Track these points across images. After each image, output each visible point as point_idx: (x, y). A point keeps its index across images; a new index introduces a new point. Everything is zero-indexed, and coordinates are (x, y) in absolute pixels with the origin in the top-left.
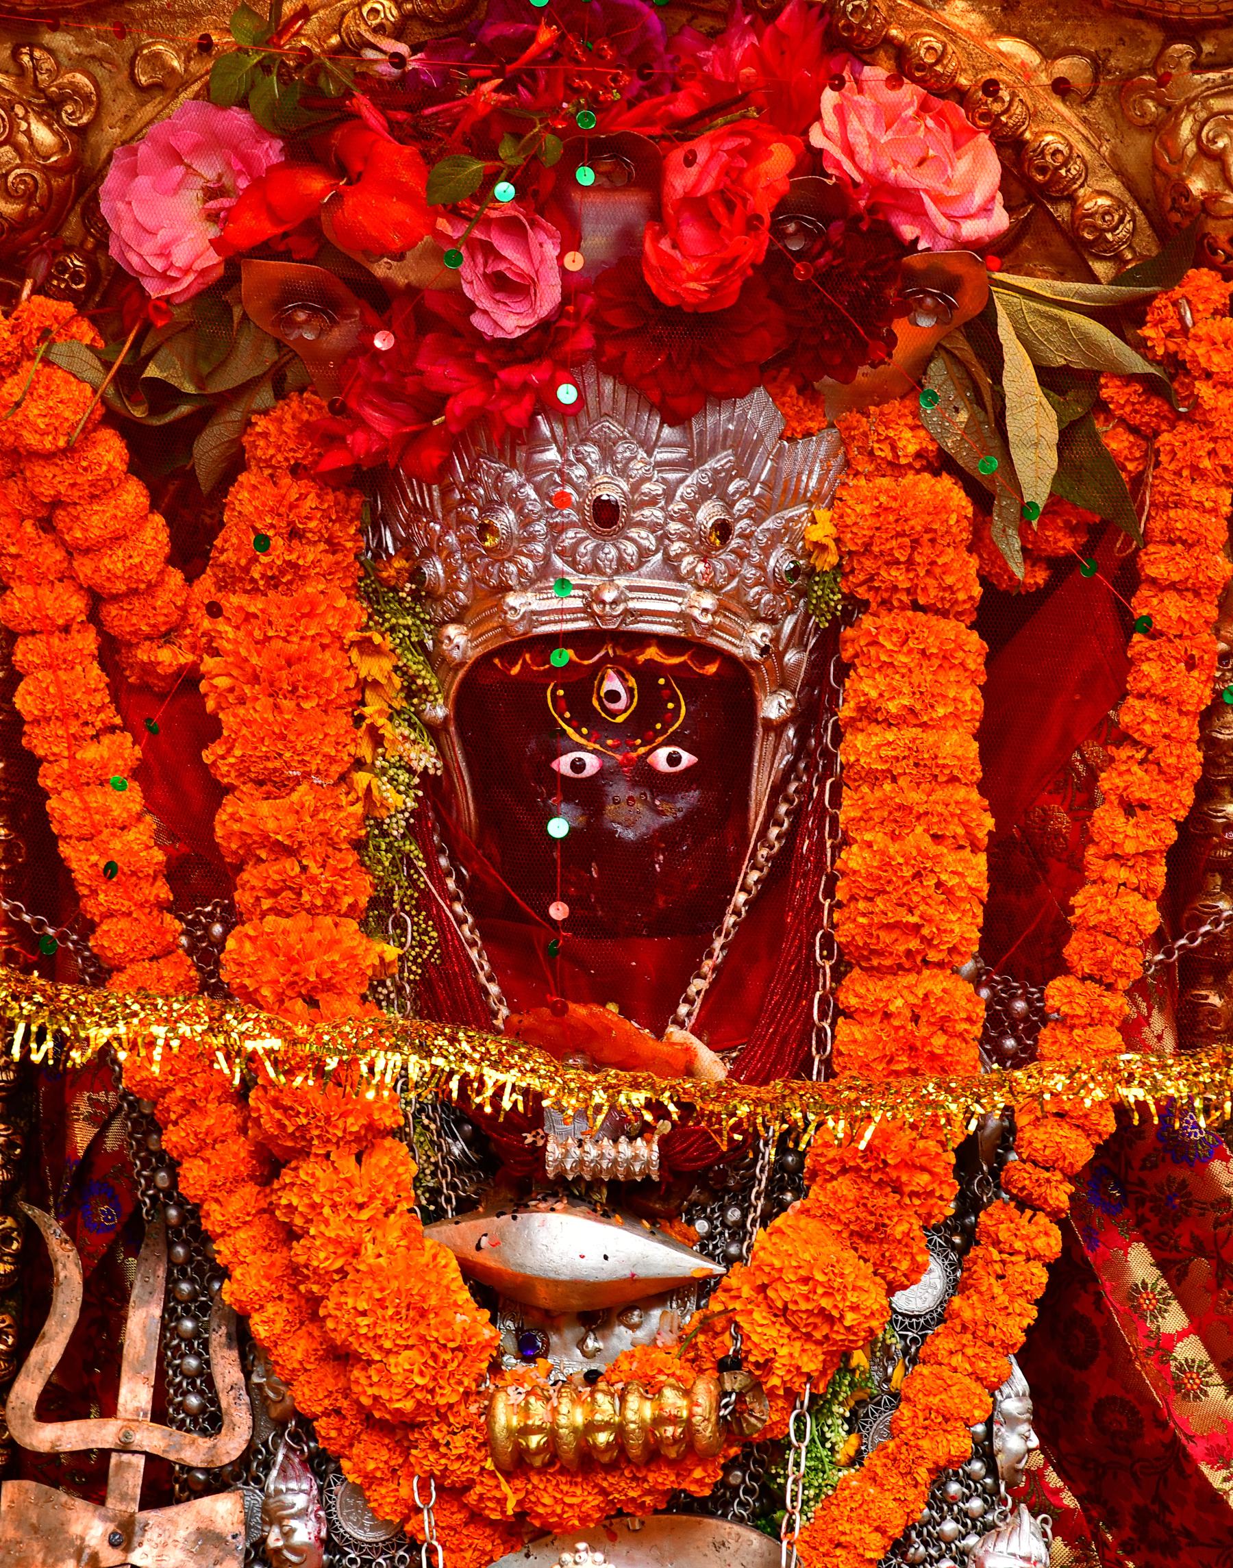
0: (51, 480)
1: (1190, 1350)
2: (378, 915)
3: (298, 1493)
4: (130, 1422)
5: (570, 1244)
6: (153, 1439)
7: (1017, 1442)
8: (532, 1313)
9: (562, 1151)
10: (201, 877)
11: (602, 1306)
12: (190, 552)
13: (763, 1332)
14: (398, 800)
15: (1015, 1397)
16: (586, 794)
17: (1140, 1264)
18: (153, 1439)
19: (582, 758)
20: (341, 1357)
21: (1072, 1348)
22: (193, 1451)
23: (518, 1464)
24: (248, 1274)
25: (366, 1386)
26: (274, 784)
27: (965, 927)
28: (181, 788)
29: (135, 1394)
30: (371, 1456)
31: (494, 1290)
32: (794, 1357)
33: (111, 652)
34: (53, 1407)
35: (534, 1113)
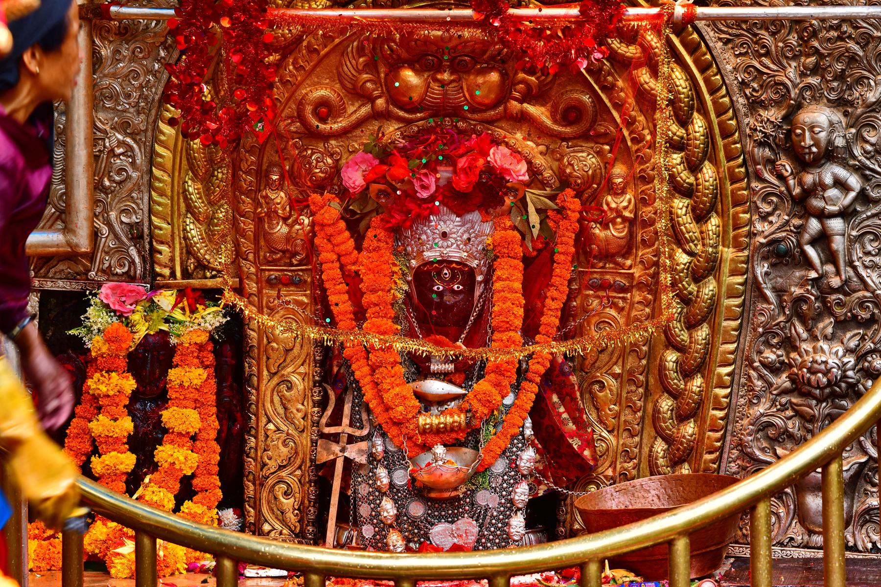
0: (329, 230)
1: (565, 416)
2: (396, 320)
3: (379, 441)
4: (345, 428)
6: (350, 430)
7: (528, 432)
8: (427, 402)
9: (434, 367)
10: (360, 315)
11: (442, 400)
12: (359, 248)
13: (476, 405)
14: (400, 296)
15: (528, 423)
16: (440, 294)
17: (555, 398)
18: (350, 430)
19: (439, 287)
20: (387, 409)
21: (540, 412)
22: (358, 433)
23: (423, 432)
24: (369, 394)
25: (392, 414)
26: (374, 291)
27: (519, 323)
28: (355, 295)
29: (346, 421)
30: (394, 431)
31: (420, 396)
32: (482, 410)
33: (342, 267)
34: (328, 425)
35: (428, 358)
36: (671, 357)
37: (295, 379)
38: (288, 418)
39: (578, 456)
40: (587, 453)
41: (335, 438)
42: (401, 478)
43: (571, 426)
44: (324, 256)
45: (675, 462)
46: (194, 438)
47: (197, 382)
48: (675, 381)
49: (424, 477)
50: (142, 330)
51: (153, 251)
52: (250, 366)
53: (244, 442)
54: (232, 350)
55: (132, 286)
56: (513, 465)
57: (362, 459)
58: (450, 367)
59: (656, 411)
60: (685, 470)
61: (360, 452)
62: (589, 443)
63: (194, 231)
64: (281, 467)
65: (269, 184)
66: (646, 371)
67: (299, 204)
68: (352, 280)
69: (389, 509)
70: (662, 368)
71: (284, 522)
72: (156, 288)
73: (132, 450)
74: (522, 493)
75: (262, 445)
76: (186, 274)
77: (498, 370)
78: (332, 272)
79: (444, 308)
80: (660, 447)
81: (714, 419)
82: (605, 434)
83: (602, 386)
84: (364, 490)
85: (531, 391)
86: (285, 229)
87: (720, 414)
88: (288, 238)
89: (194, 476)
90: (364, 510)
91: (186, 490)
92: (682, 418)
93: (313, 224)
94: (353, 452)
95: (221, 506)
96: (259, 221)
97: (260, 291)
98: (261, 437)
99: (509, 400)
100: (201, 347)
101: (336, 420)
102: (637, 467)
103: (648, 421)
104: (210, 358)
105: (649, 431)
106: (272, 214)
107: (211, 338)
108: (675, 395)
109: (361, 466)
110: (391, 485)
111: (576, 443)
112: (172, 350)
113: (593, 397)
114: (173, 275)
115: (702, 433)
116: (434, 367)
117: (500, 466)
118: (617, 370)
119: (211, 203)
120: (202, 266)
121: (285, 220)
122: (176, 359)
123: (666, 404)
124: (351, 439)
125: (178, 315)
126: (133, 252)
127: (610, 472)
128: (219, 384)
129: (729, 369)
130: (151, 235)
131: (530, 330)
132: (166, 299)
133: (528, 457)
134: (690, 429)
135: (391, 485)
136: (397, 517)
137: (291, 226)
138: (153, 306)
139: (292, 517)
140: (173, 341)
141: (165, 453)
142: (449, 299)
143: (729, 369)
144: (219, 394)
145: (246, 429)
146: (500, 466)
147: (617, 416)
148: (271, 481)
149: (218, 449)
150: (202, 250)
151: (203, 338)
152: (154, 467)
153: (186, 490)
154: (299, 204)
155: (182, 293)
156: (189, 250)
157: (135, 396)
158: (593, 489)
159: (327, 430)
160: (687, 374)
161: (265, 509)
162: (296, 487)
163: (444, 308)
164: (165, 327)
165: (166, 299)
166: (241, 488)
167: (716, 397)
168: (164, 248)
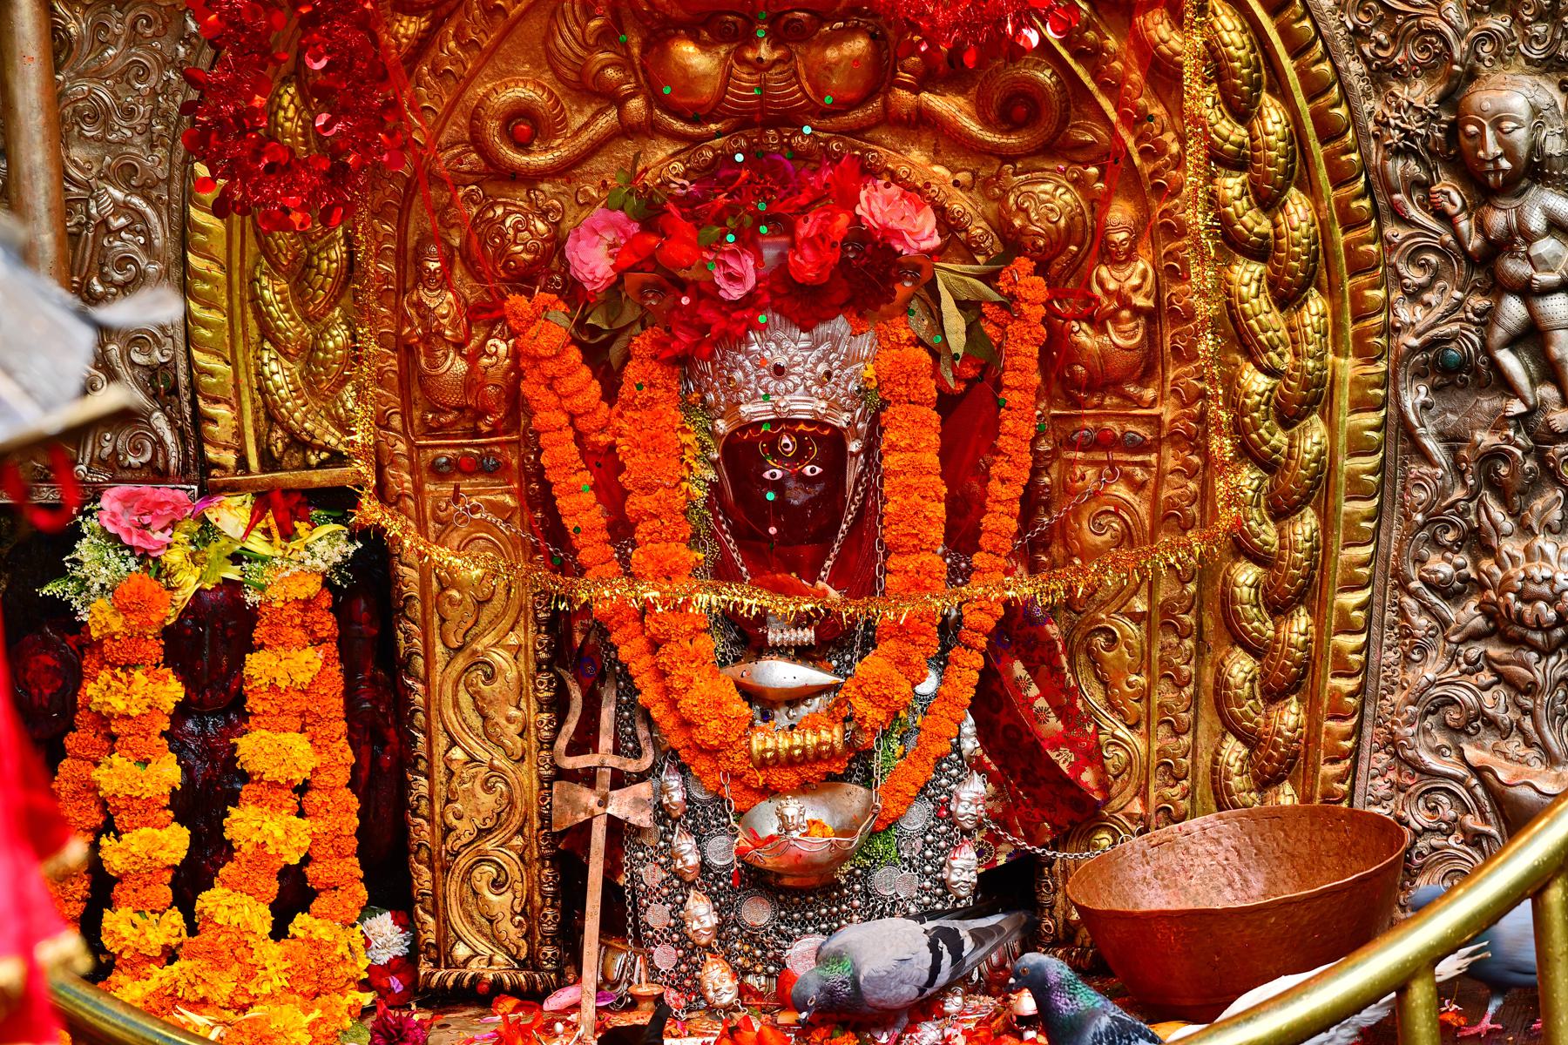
0: (550, 368)
1: (1041, 703)
2: (694, 541)
3: (674, 781)
4: (604, 756)
5: (782, 673)
6: (614, 761)
7: (970, 744)
8: (765, 702)
9: (773, 637)
10: (621, 530)
12: (610, 394)
13: (861, 706)
14: (700, 493)
15: (969, 726)
16: (778, 486)
17: (1019, 669)
18: (614, 761)
21: (992, 703)
22: (632, 766)
23: (763, 764)
24: (649, 693)
25: (699, 736)
26: (648, 489)
27: (937, 533)
28: (611, 493)
29: (606, 742)
30: (703, 764)
31: (750, 694)
33: (579, 438)
34: (572, 750)
35: (762, 619)
36: (1246, 575)
37: (499, 658)
38: (489, 734)
39: (1069, 784)
40: (1087, 776)
41: (588, 778)
42: (720, 851)
43: (1054, 724)
44: (541, 418)
45: (1266, 782)
46: (303, 789)
47: (304, 678)
48: (1261, 625)
49: (768, 860)
50: (189, 582)
51: (199, 418)
52: (408, 638)
53: (405, 787)
54: (367, 603)
55: (164, 492)
56: (943, 813)
57: (643, 819)
58: (808, 635)
59: (1221, 683)
60: (1286, 796)
61: (638, 802)
62: (1092, 755)
63: (280, 374)
64: (483, 833)
65: (423, 278)
66: (1197, 604)
67: (486, 314)
68: (605, 465)
69: (702, 914)
70: (1227, 600)
71: (495, 940)
72: (209, 492)
73: (180, 819)
74: (964, 867)
75: (441, 790)
76: (269, 462)
77: (901, 632)
78: (560, 452)
80: (1233, 751)
81: (1337, 695)
82: (1122, 732)
83: (1112, 641)
84: (652, 875)
85: (969, 666)
86: (461, 366)
87: (1348, 685)
88: (472, 383)
89: (307, 860)
90: (657, 916)
91: (293, 894)
92: (1274, 694)
93: (515, 354)
94: (622, 805)
95: (367, 911)
96: (407, 351)
97: (418, 488)
98: (440, 775)
99: (928, 686)
100: (307, 604)
101: (585, 741)
102: (1189, 793)
103: (1206, 702)
104: (327, 625)
105: (1208, 721)
106: (432, 337)
107: (327, 583)
108: (1256, 649)
109: (639, 831)
110: (704, 867)
111: (1063, 759)
112: (251, 617)
113: (1095, 661)
114: (242, 463)
115: (1313, 723)
116: (773, 637)
117: (917, 817)
118: (1140, 606)
119: (309, 319)
120: (299, 443)
121: (459, 346)
122: (259, 634)
123: (1240, 667)
124: (620, 780)
125: (257, 544)
126: (160, 421)
127: (1136, 807)
128: (349, 675)
129: (1361, 596)
130: (194, 388)
131: (963, 535)
132: (232, 515)
133: (972, 795)
134: (1290, 715)
135: (704, 867)
136: (720, 928)
137: (472, 359)
138: (207, 532)
139: (510, 930)
140: (251, 597)
141: (246, 823)
143: (1361, 596)
144: (350, 695)
145: (406, 761)
146: (917, 817)
147: (1145, 695)
148: (463, 862)
149: (354, 803)
150: (298, 413)
151: (312, 587)
152: (227, 850)
153: (293, 894)
154: (486, 314)
155: (263, 501)
156: (270, 414)
157: (182, 711)
158: (1104, 839)
159: (569, 763)
160: (1279, 608)
161: (455, 916)
162: (514, 870)
164: (233, 573)
165: (232, 515)
166: (406, 879)
167: (1338, 652)
168: (221, 411)
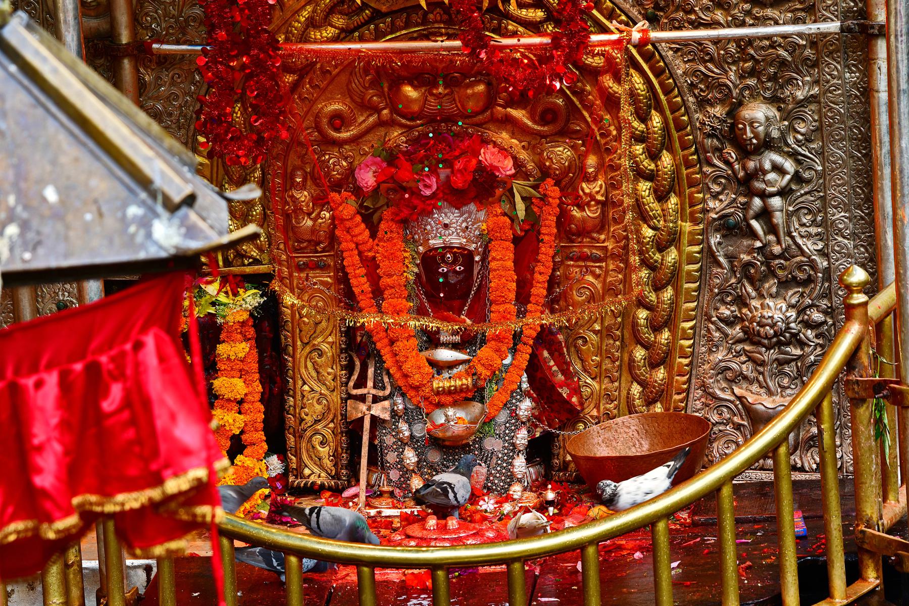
79: (449, 287)
142: (453, 280)
163: (449, 287)
